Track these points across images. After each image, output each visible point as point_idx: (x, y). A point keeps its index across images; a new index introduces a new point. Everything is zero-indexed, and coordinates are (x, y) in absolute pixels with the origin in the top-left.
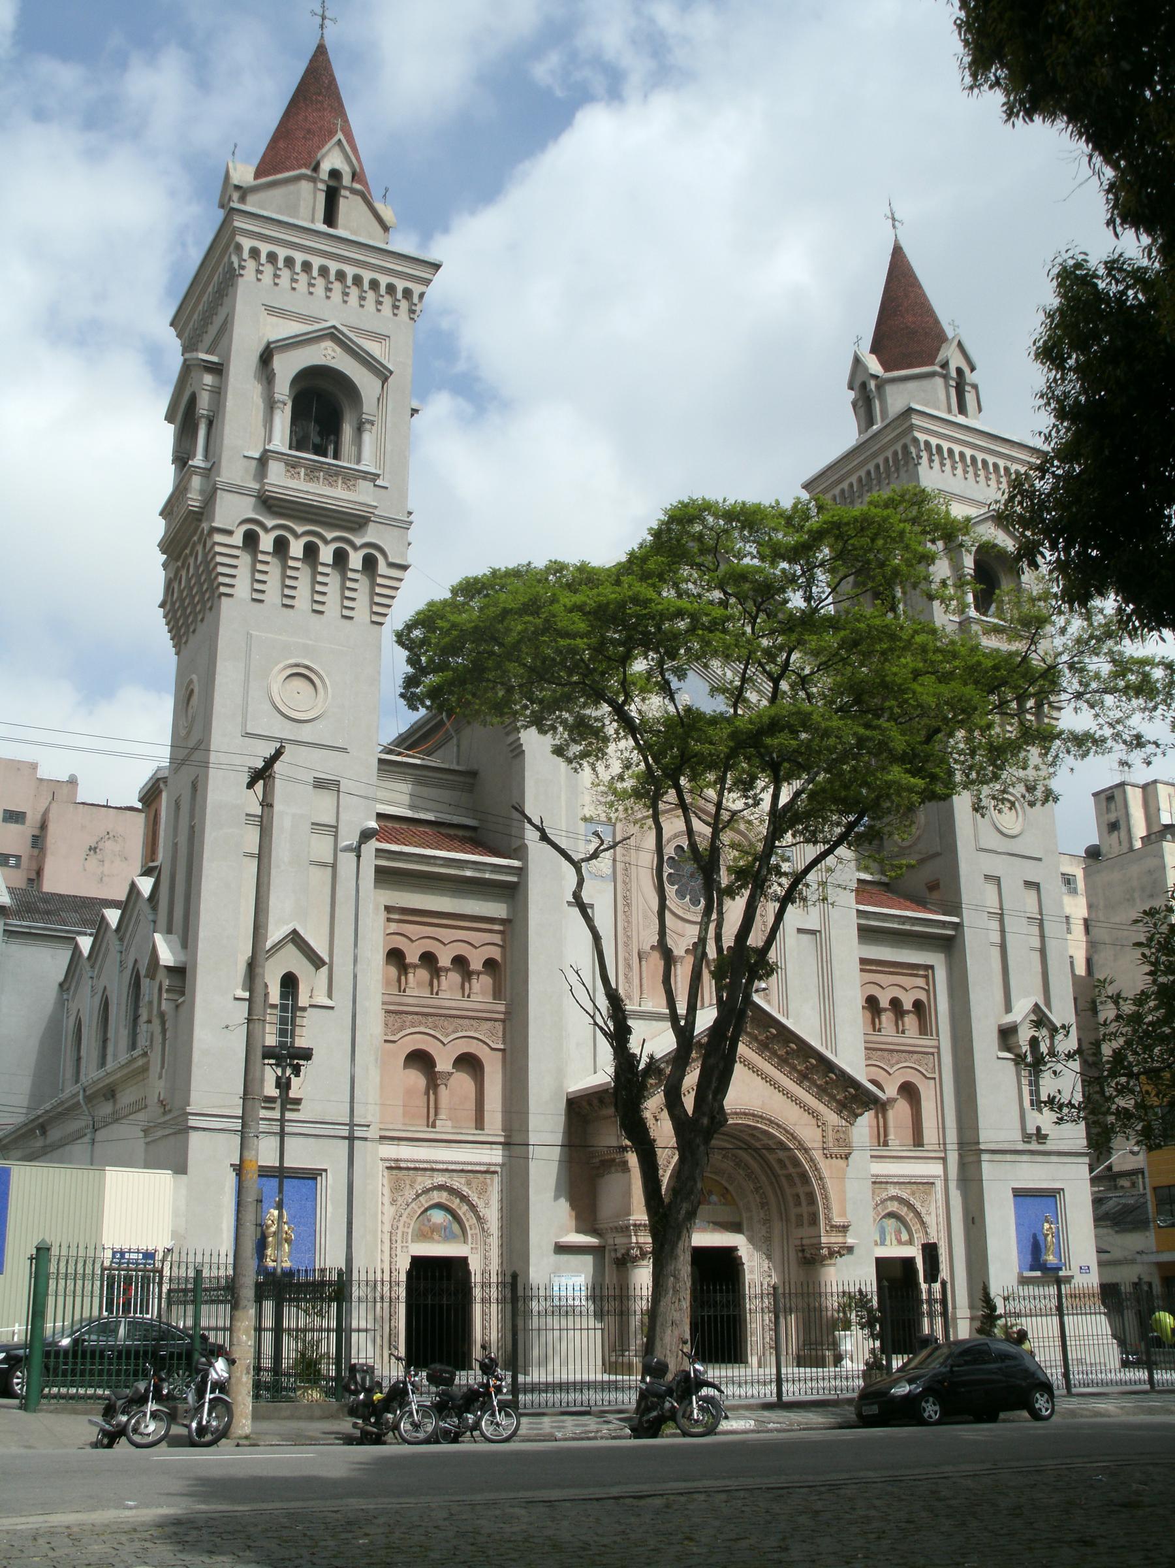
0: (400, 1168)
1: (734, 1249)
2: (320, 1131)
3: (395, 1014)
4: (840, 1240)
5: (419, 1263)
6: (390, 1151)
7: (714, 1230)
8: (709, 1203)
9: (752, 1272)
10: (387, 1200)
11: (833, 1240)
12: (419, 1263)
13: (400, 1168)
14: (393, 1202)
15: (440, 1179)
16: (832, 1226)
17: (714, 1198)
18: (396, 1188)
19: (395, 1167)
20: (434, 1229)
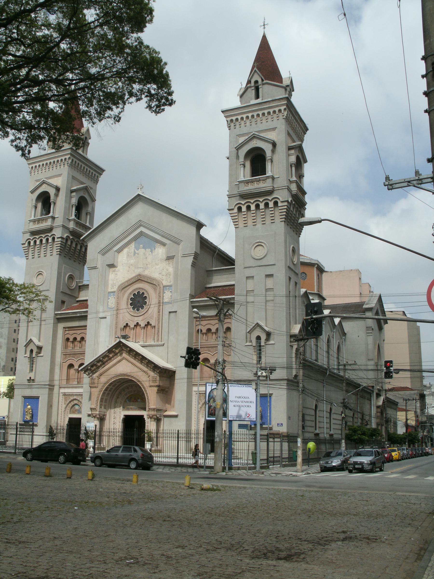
0: (65, 395)
1: (143, 416)
2: (42, 386)
3: (65, 355)
4: (153, 413)
5: (70, 419)
6: (62, 390)
7: (139, 410)
8: (138, 402)
9: (148, 423)
10: (63, 403)
11: (150, 413)
12: (70, 419)
13: (65, 395)
14: (65, 404)
15: (75, 397)
16: (149, 409)
17: (139, 400)
18: (66, 400)
19: (65, 394)
20: (76, 410)
